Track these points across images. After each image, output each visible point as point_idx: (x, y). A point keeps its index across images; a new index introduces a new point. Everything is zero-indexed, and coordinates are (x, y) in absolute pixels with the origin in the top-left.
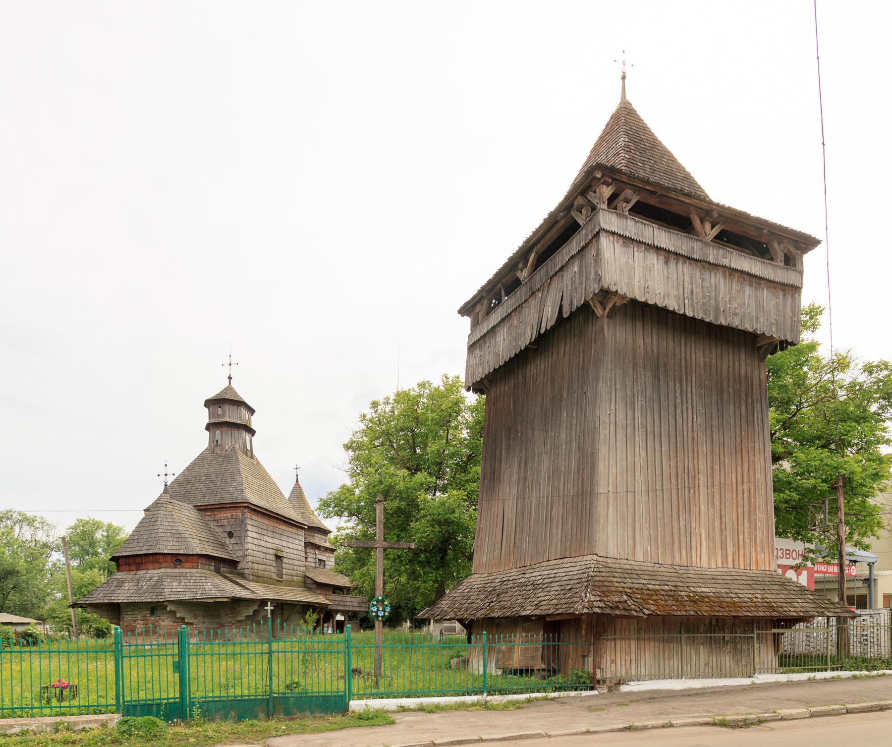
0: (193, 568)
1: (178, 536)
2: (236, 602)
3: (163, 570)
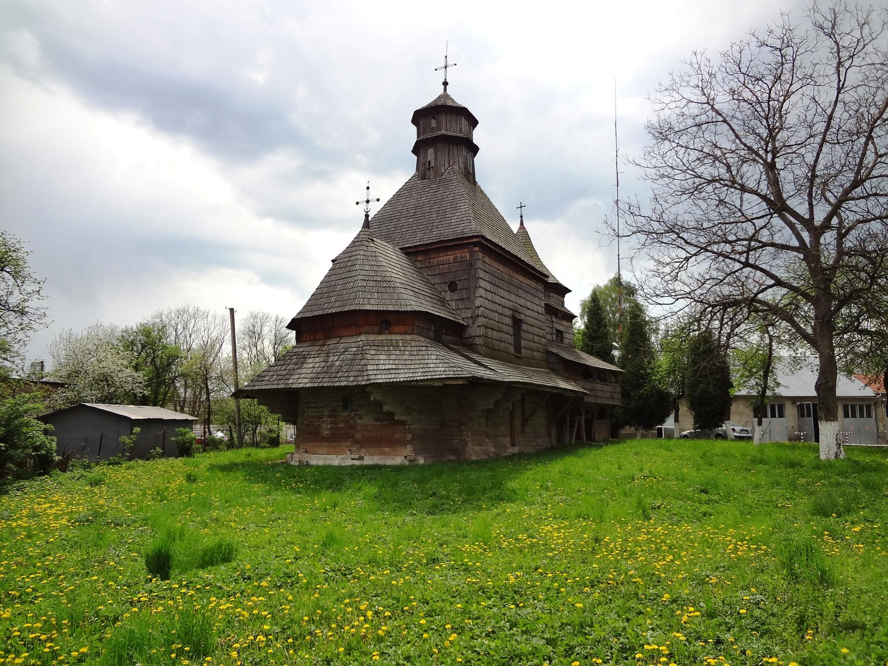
0: (406, 333)
1: (384, 285)
2: (475, 383)
3: (363, 337)
